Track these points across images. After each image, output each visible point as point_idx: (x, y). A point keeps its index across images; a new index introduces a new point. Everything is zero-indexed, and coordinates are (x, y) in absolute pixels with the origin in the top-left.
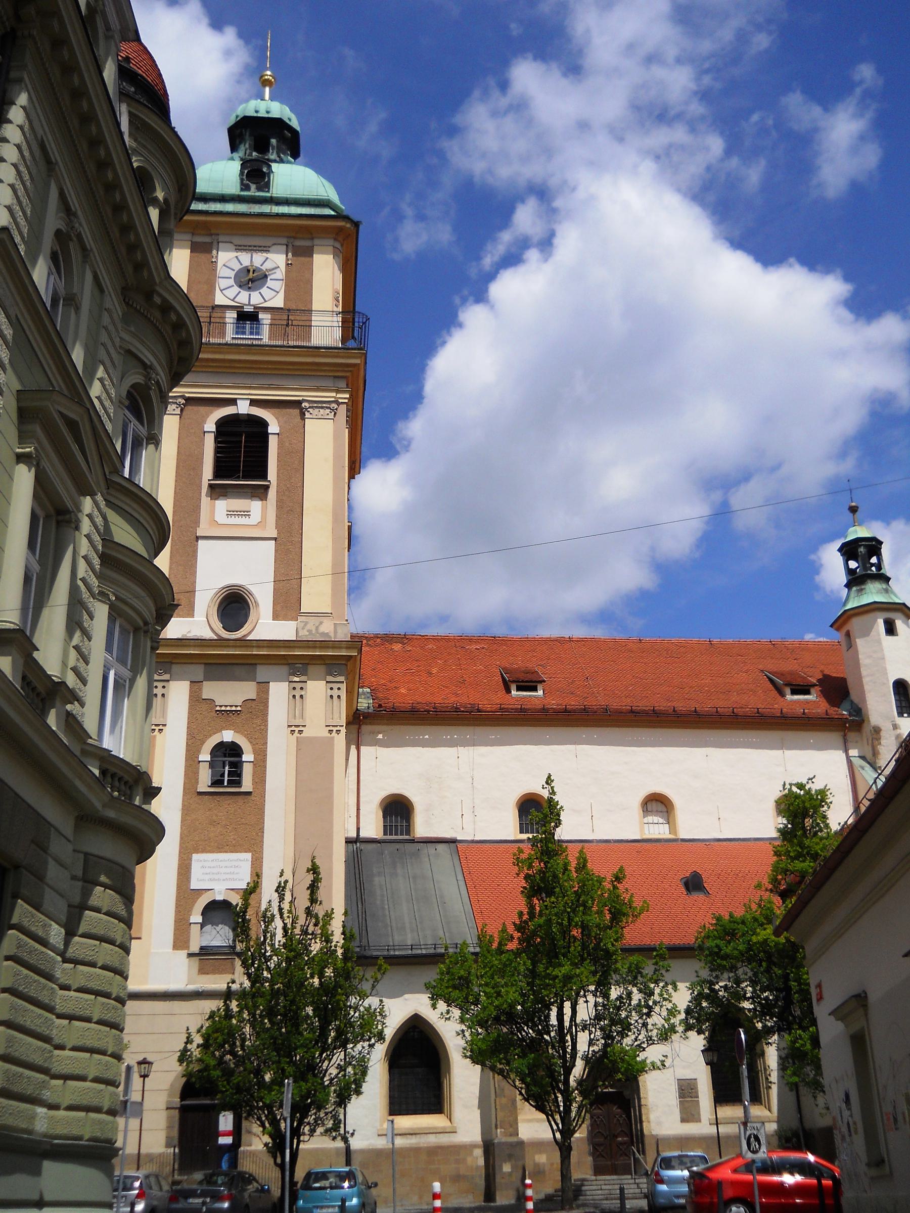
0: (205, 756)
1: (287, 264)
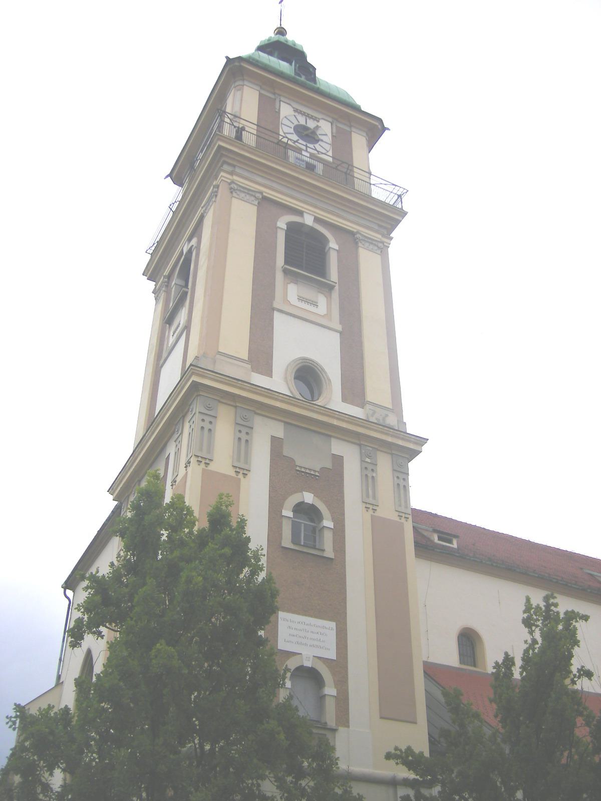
0: (288, 513)
1: (333, 136)
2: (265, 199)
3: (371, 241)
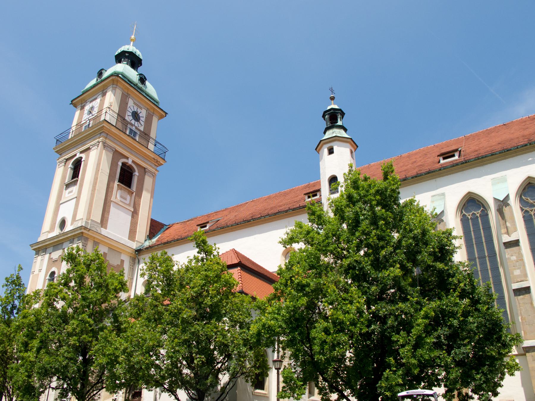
1: (146, 117)
2: (116, 150)
3: (150, 172)
